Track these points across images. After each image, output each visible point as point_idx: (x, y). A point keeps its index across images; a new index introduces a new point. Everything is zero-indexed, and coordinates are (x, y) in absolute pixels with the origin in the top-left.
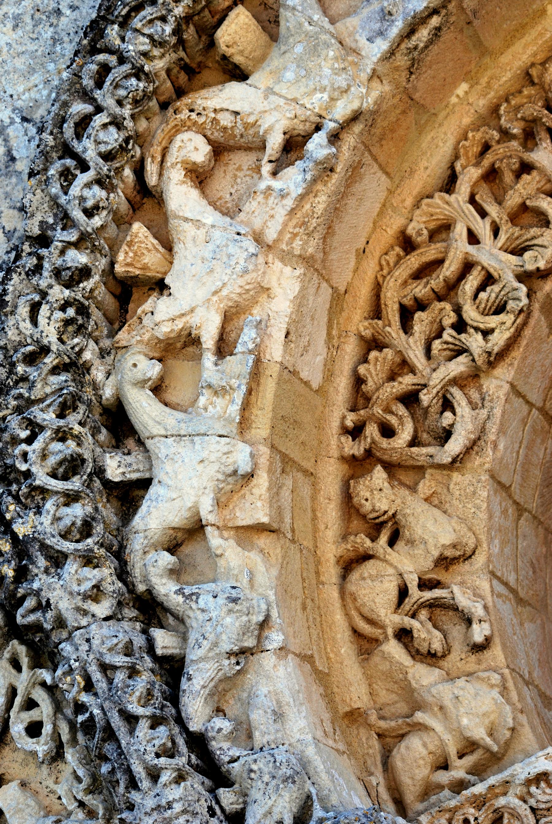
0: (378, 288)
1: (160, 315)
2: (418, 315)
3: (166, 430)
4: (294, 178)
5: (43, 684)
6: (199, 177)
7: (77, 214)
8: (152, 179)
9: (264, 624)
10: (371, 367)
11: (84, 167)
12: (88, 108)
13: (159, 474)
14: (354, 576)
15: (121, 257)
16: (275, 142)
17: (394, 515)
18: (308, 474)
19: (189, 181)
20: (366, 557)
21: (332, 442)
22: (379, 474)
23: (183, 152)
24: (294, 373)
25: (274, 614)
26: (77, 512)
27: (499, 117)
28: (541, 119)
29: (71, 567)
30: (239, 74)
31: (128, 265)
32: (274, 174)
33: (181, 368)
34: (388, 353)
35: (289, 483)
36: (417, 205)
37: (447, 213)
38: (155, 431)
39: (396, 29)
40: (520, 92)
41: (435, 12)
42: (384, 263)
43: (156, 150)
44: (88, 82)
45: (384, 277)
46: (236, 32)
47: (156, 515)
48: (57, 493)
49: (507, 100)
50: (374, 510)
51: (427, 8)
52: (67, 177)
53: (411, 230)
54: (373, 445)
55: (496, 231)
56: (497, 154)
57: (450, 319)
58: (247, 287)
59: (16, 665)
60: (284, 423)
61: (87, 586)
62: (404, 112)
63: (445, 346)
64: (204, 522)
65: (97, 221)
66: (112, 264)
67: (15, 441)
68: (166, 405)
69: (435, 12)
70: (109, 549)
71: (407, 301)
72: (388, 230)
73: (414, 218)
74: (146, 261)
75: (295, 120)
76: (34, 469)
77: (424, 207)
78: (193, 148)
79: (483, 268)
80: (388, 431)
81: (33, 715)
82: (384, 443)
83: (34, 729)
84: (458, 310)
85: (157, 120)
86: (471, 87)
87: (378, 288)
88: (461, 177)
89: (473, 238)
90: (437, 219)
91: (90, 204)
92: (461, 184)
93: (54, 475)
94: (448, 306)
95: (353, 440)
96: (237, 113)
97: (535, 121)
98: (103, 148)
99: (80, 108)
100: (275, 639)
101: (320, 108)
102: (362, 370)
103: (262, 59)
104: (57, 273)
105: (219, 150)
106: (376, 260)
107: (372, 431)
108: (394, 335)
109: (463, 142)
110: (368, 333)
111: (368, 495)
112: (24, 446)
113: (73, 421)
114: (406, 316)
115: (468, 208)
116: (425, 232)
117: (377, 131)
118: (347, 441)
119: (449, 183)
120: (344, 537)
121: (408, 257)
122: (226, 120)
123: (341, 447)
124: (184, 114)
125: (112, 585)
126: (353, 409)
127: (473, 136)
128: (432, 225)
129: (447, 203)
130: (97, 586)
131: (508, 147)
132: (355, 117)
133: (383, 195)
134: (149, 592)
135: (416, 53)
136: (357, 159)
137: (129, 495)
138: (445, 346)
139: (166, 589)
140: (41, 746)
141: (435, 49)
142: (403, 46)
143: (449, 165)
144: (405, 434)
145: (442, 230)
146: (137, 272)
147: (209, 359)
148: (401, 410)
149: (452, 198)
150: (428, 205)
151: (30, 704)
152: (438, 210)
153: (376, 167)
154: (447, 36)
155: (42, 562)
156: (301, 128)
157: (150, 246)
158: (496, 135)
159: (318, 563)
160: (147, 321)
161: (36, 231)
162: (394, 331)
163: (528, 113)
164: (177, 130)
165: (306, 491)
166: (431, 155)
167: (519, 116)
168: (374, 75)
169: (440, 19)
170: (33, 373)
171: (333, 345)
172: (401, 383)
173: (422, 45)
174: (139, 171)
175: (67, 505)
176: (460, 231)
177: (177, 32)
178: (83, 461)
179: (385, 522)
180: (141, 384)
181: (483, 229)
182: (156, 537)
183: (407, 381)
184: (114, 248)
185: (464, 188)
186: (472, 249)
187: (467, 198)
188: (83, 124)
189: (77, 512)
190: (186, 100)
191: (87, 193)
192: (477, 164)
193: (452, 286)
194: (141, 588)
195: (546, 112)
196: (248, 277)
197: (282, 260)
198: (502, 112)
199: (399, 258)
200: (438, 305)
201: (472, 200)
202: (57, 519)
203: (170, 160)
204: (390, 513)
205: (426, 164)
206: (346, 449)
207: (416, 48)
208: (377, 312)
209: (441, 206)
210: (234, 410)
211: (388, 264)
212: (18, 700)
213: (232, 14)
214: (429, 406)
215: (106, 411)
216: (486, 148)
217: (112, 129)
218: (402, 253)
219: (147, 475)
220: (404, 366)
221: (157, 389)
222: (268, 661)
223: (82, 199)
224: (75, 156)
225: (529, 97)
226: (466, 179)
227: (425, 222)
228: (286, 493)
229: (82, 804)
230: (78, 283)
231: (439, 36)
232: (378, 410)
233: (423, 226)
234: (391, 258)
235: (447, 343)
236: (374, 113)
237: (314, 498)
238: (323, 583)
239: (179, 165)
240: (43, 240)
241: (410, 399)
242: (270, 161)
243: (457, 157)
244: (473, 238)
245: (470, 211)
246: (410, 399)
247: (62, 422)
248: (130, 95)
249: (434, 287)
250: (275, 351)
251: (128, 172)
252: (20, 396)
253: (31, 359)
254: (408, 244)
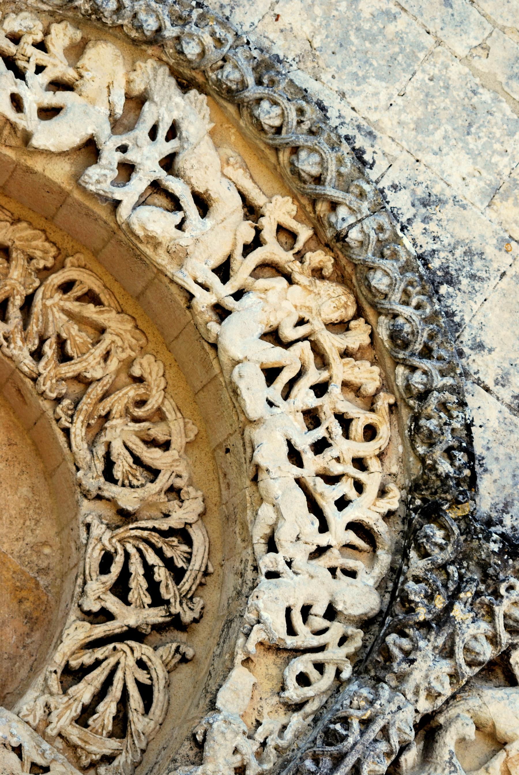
5: (338, 672)
29: (445, 667)
48: (494, 628)
59: (343, 640)
61: (438, 688)
76: (505, 601)
81: (313, 674)
83: (303, 680)
134: (440, 727)
140: (294, 692)
151: (320, 667)
155: (440, 641)
182: (483, 715)
194: (441, 720)
212: (319, 657)
229: (264, 744)
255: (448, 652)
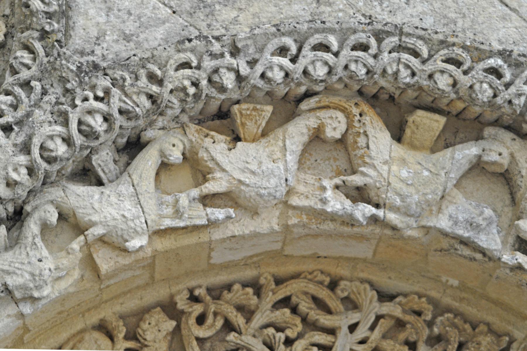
0: (296, 276)
1: (216, 148)
2: (287, 311)
3: (138, 184)
4: (337, 203)
6: (317, 137)
7: (259, 69)
8: (304, 106)
9: (33, 300)
10: (241, 292)
11: (294, 60)
12: (335, 47)
13: (107, 190)
14: (97, 335)
15: (244, 106)
16: (357, 180)
17: (146, 346)
18: (152, 277)
19: (312, 132)
20: (111, 338)
21: (180, 286)
22: (171, 324)
23: (329, 121)
24: (211, 250)
25: (43, 302)
26: (60, 149)
27: (442, 315)
28: (450, 344)
29: (22, 159)
30: (398, 137)
31: (241, 113)
32: (337, 187)
33: (185, 175)
34: (254, 300)
35: (138, 273)
36: (363, 281)
37: (364, 303)
38: (134, 177)
39: (462, 232)
40: (465, 322)
41: (484, 254)
42: (315, 273)
43: (325, 101)
44: (353, 39)
45: (305, 278)
46: (425, 124)
47: (81, 197)
48: (68, 130)
49: (456, 316)
50: (144, 331)
51: (483, 248)
52: (283, 51)
53: (343, 284)
54: (188, 314)
55: (363, 342)
56: (416, 323)
57: (291, 333)
58: (252, 200)
60: (175, 255)
61: (14, 176)
62: (416, 253)
63: (272, 337)
64: (86, 233)
65: (260, 83)
66: (238, 102)
67: (93, 88)
68: (157, 174)
69: (484, 254)
70: (45, 177)
71: (294, 299)
72: (339, 268)
73: (353, 283)
74: (248, 123)
75: (376, 189)
77: (362, 287)
78: (335, 126)
79: (334, 343)
80: (201, 320)
82: (192, 321)
84: (300, 336)
85: (348, 92)
86: (457, 288)
87: (296, 276)
88: (392, 304)
89: (353, 328)
90: (358, 299)
91: (269, 74)
92: (387, 306)
93: (80, 123)
94: (300, 327)
95: (188, 299)
96: (368, 147)
97: (448, 341)
98: (310, 68)
99: (333, 41)
100: (27, 309)
101: (389, 203)
102: (237, 287)
103: (413, 147)
104: (216, 71)
105: (342, 141)
106: (315, 268)
107: (198, 309)
108: (268, 299)
109: (416, 297)
110: (262, 281)
111: (153, 323)
112: (91, 95)
113: (119, 120)
114: (285, 302)
115: (371, 317)
116: (346, 294)
117: (393, 242)
118: (186, 295)
119: (385, 297)
120: (122, 317)
121: (325, 288)
122: (362, 141)
123: (179, 292)
124: (355, 111)
125: (22, 192)
126: (209, 290)
127: (423, 302)
128: (352, 296)
129: (371, 302)
130: (16, 183)
131: (423, 329)
132: (394, 228)
133: (361, 255)
135: (452, 251)
136: (369, 237)
137: (86, 174)
138: (272, 337)
139: (32, 227)
141: (462, 260)
142: (453, 241)
143: (399, 292)
144: (202, 332)
145: (351, 304)
146: (239, 121)
147: (195, 193)
148: (220, 323)
149: (376, 304)
150: (365, 289)
152: (364, 297)
153: (374, 247)
154: (474, 265)
155: (20, 139)
156: (372, 194)
157: (259, 123)
158: (429, 317)
159: (96, 307)
160: (208, 140)
161: (240, 45)
162: (270, 298)
163: (451, 334)
164: (343, 110)
165: (140, 282)
166: (401, 278)
167: (447, 328)
168: (427, 230)
169: (482, 258)
170: (143, 81)
171: (246, 263)
172: (236, 316)
173: (460, 253)
174: (308, 95)
175: (64, 140)
176: (354, 317)
177: (408, 85)
178: (97, 138)
179: (140, 342)
180: (162, 154)
181: (361, 333)
182: (65, 205)
183: (239, 320)
184: (250, 98)
185: (387, 308)
186: (345, 329)
187: (379, 313)
188: (324, 47)
189: (60, 149)
190: (365, 107)
191: (276, 69)
192: (404, 311)
193: (315, 326)
195: (456, 346)
196: (258, 198)
197: (281, 214)
198: (446, 315)
199: (321, 283)
200: (298, 321)
201: (379, 318)
202: (51, 137)
203: (322, 114)
204: (146, 343)
205: (393, 277)
206: (179, 297)
207: (456, 249)
208: (279, 281)
209: (368, 298)
210: (168, 223)
211: (316, 277)
213: (437, 117)
214: (227, 342)
215: (139, 137)
216: (419, 314)
217: (326, 70)
218: (326, 283)
219: (105, 181)
220: (248, 313)
221: (164, 166)
222: (12, 309)
223: (271, 68)
224: (300, 50)
225: (465, 330)
226: (392, 308)
227: (353, 291)
228: (130, 274)
230: (214, 87)
231: (471, 261)
232: (212, 308)
233: (350, 290)
234: (320, 277)
235: (274, 338)
236: (402, 238)
237: (138, 288)
238: (83, 316)
239: (319, 122)
240: (235, 52)
241: (229, 327)
242: (344, 182)
243: (405, 295)
244: (353, 328)
245: (370, 319)
246: (229, 327)
247: (116, 115)
248: (353, 73)
249: (310, 314)
250: (217, 235)
251: (303, 89)
252: (124, 80)
253: (152, 77)
254: (333, 286)
255: (26, 149)
